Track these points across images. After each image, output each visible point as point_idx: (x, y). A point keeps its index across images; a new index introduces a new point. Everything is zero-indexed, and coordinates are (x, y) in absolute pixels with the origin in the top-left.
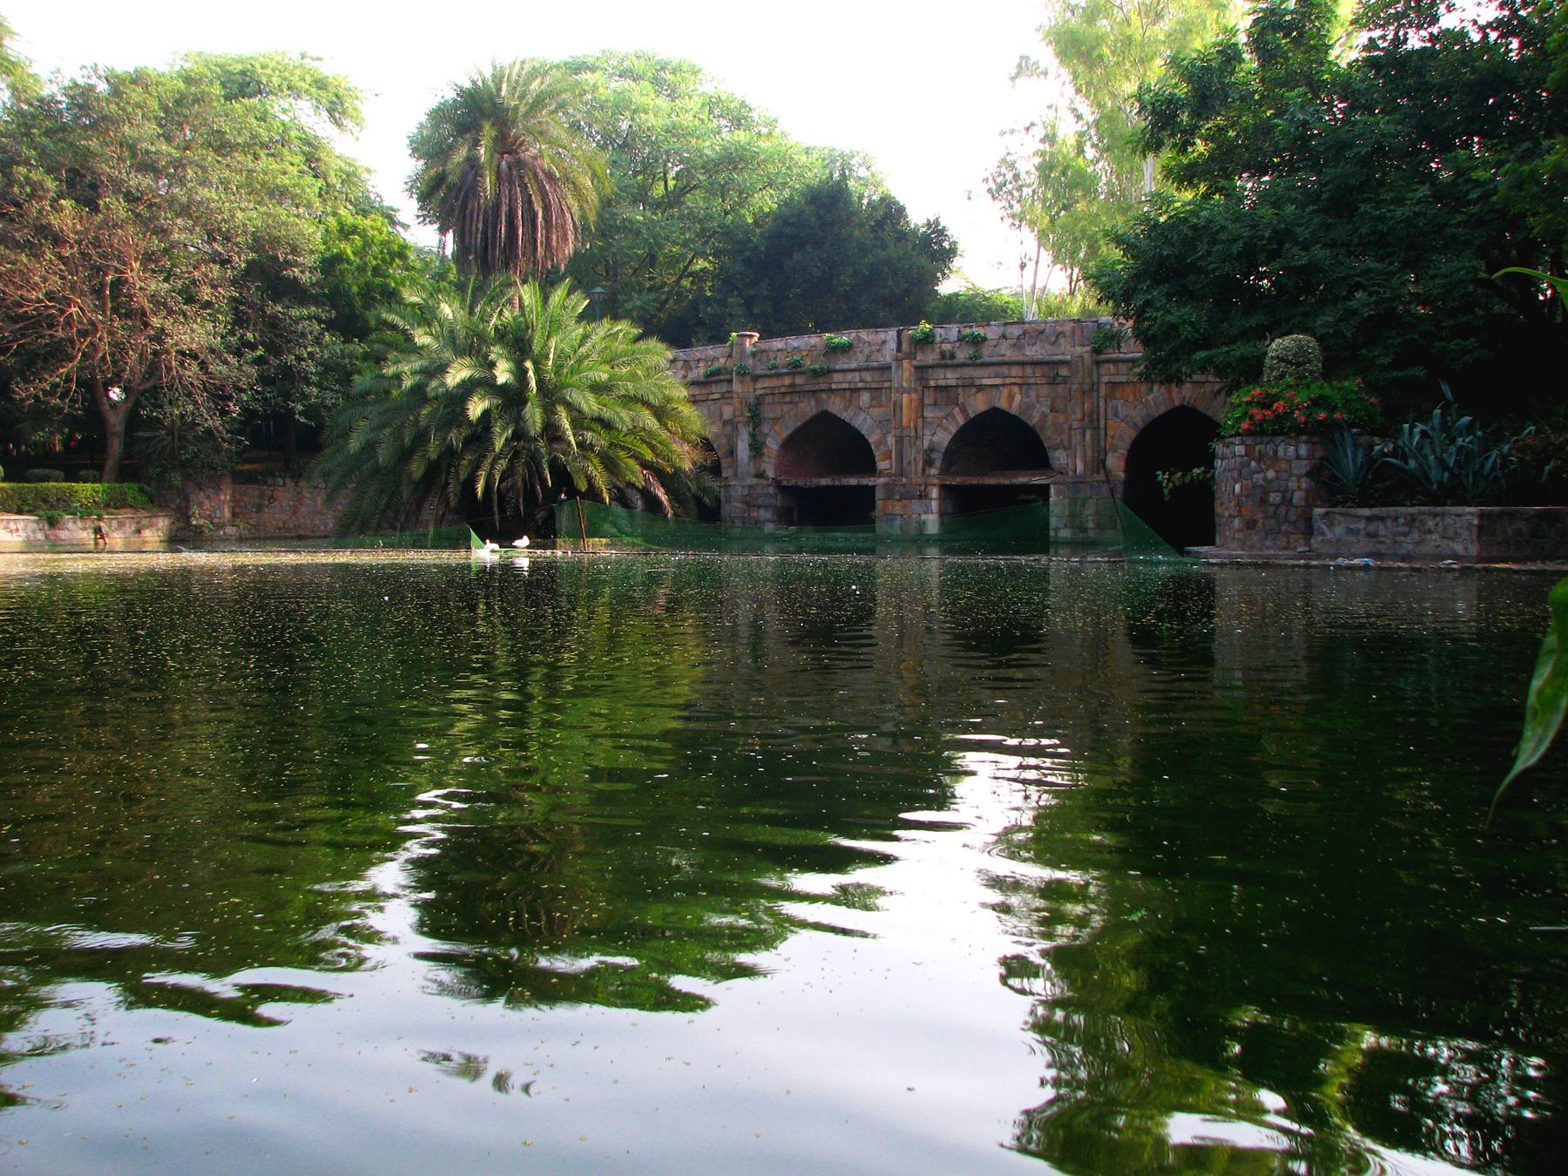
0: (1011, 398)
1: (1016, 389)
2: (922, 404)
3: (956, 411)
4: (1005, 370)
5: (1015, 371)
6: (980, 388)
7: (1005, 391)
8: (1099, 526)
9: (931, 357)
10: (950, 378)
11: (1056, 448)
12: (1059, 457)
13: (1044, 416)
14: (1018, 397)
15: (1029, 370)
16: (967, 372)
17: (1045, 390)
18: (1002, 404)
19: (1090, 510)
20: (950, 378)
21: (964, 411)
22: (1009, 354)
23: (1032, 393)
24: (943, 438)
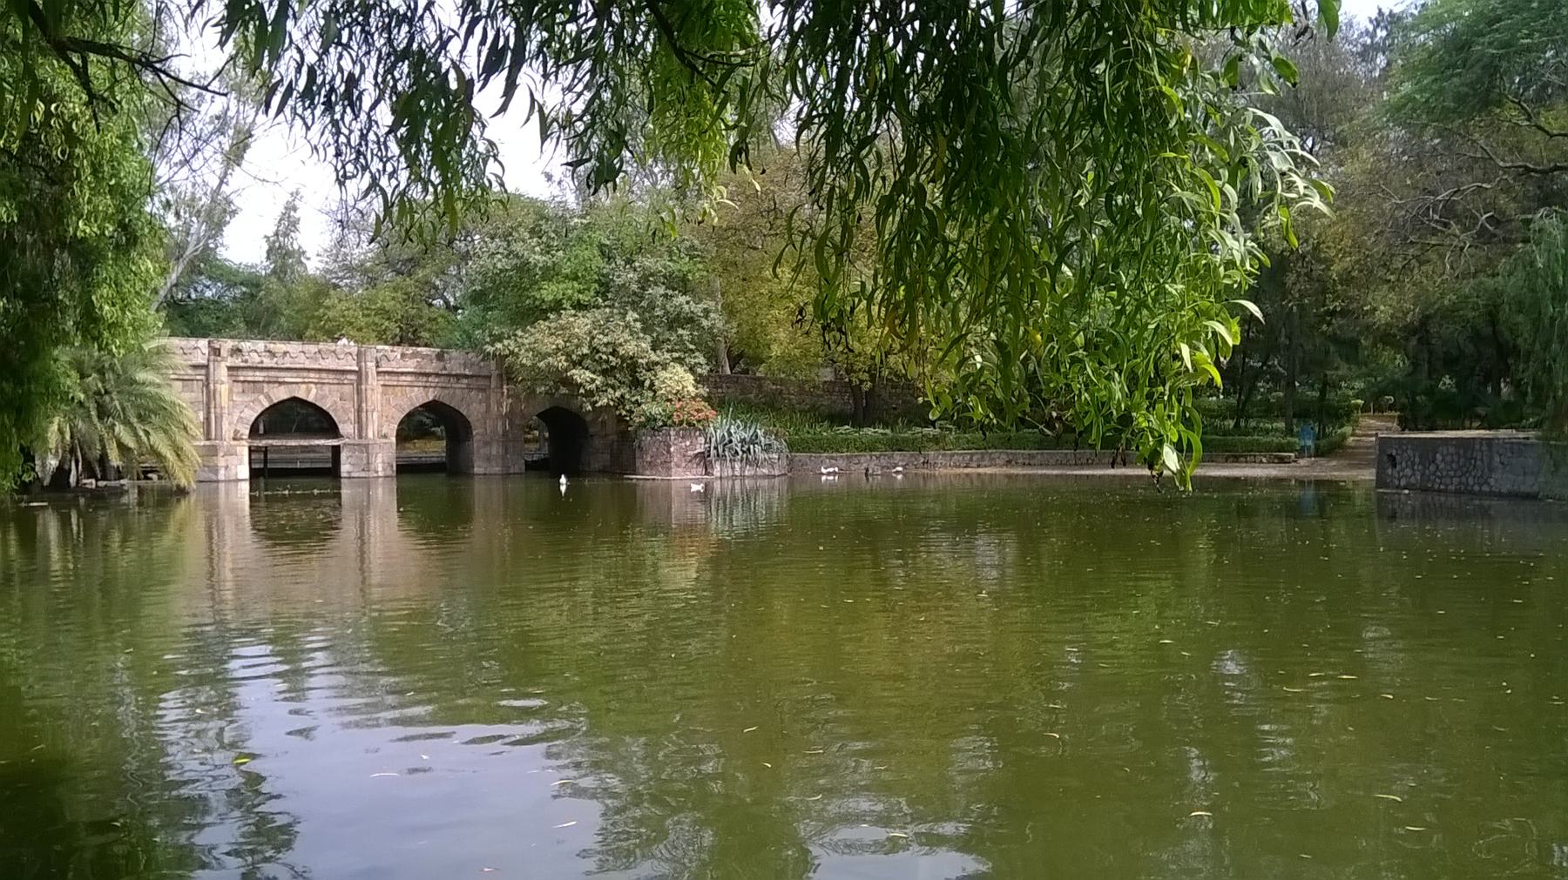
0: (309, 391)
2: (231, 391)
3: (262, 397)
9: (238, 362)
10: (259, 376)
12: (346, 428)
14: (314, 391)
15: (324, 375)
16: (272, 373)
19: (379, 460)
21: (268, 397)
22: (308, 365)
24: (251, 415)
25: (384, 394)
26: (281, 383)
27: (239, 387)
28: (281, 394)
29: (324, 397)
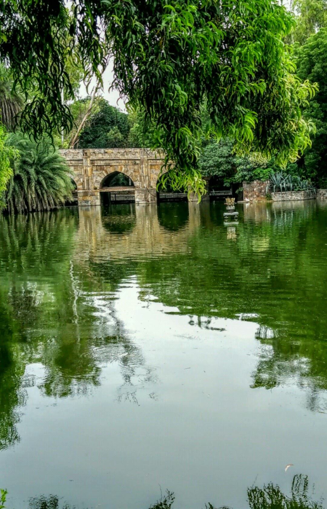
0: (121, 168)
1: (123, 166)
2: (92, 170)
3: (104, 172)
4: (120, 161)
5: (123, 161)
6: (111, 166)
7: (119, 167)
8: (151, 200)
10: (102, 163)
11: (136, 181)
12: (137, 184)
13: (132, 173)
14: (123, 169)
15: (127, 161)
16: (107, 162)
17: (132, 166)
18: (118, 170)
19: (149, 196)
20: (102, 163)
21: (106, 172)
22: (121, 157)
23: (128, 167)
24: (100, 179)
25: (151, 168)
26: (111, 166)
27: (95, 168)
28: (111, 170)
29: (127, 171)
